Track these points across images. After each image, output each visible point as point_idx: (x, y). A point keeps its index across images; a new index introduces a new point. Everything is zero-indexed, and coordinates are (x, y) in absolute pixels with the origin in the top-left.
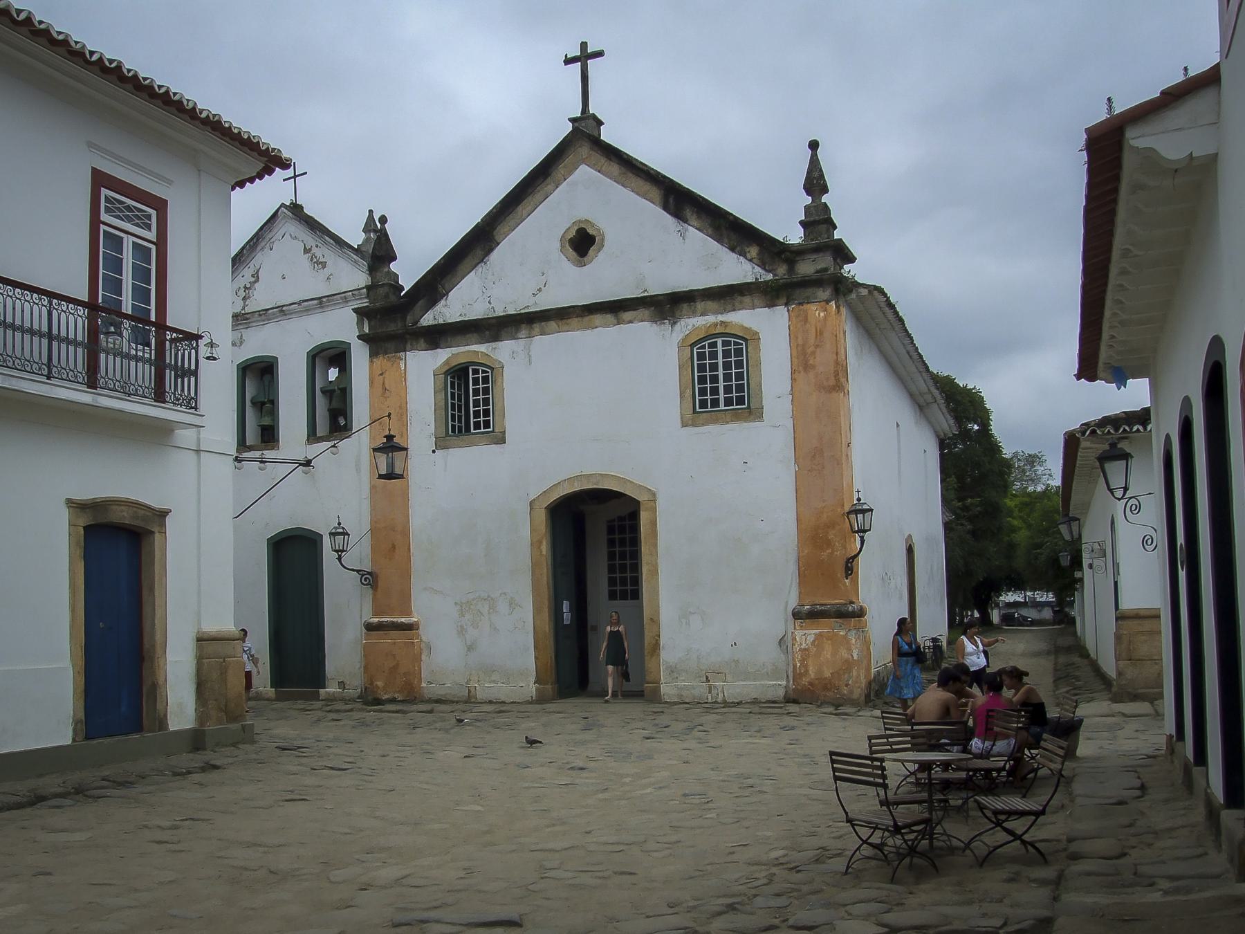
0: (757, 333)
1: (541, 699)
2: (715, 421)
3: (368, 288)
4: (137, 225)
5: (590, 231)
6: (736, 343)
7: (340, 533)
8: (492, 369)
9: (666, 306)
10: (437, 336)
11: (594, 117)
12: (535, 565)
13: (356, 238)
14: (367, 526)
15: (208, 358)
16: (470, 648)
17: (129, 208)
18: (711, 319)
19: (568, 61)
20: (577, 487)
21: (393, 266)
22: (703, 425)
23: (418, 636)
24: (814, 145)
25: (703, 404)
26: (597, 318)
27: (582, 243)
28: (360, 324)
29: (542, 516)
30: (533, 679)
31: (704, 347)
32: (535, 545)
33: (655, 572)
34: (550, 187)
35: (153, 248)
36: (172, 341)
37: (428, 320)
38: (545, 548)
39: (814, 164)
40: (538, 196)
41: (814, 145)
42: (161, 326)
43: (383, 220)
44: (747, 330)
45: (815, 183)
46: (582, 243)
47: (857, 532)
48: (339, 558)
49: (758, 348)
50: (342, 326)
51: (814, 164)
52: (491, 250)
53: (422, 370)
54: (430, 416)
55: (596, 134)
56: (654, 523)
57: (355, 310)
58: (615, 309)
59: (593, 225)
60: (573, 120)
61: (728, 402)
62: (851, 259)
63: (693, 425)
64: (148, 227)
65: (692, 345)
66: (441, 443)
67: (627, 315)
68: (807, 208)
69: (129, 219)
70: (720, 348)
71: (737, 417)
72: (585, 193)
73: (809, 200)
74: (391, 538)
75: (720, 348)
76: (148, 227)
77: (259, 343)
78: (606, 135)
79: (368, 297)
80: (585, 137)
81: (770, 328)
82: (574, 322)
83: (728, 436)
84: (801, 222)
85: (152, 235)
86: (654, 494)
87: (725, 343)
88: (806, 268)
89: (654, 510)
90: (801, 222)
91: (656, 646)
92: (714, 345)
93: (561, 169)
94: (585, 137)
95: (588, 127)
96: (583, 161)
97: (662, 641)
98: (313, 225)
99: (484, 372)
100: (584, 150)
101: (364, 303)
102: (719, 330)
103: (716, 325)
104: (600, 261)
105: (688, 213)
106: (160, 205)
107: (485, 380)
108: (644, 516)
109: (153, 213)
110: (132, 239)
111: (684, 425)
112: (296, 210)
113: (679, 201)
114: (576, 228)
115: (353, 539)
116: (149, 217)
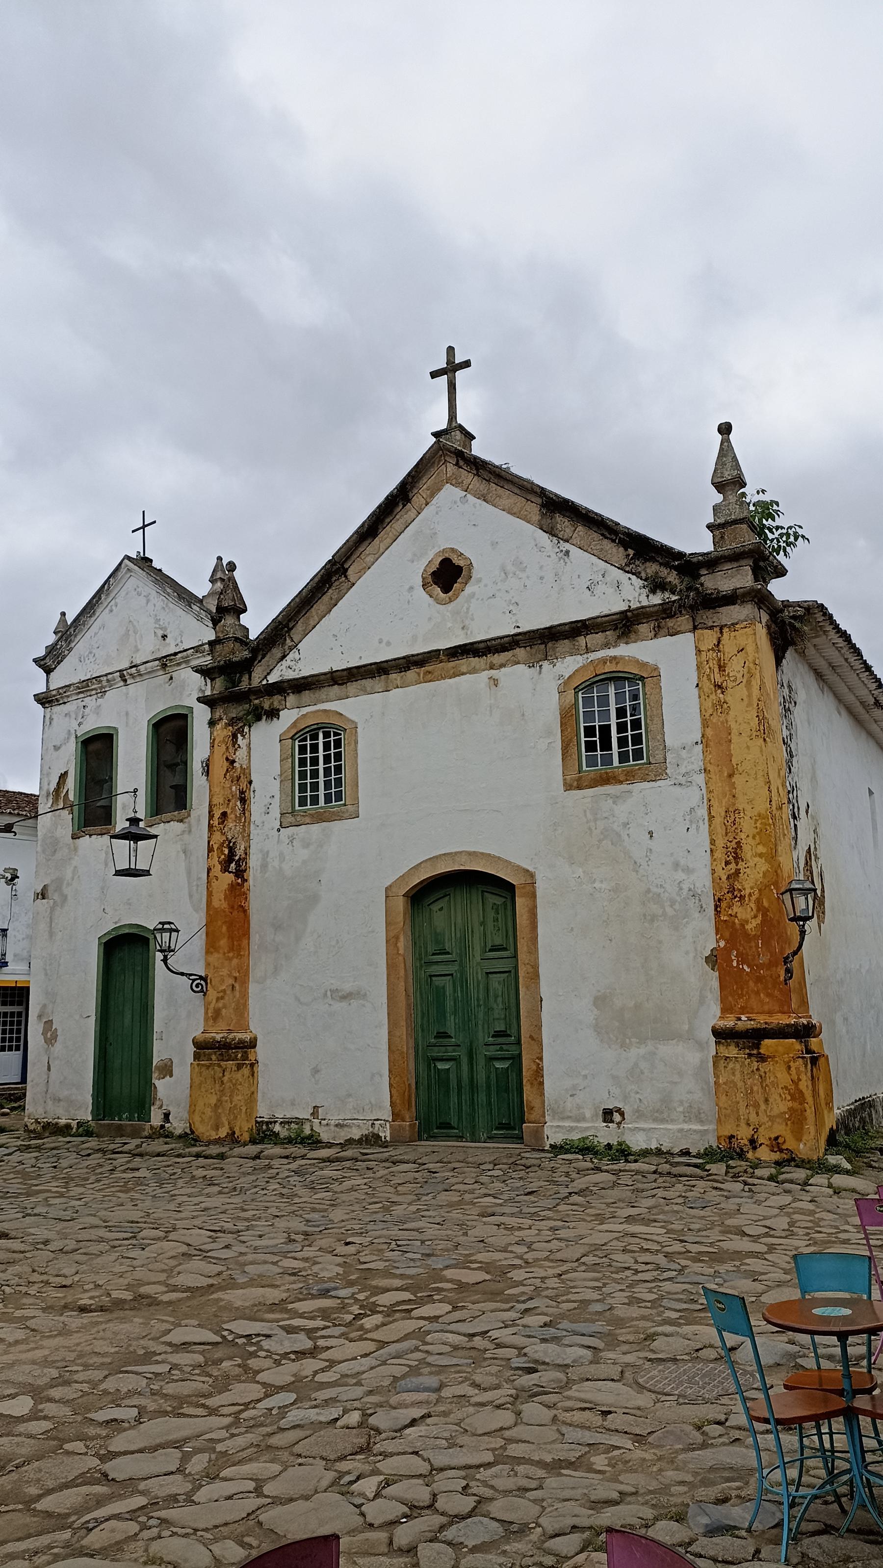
5: (456, 561)
11: (461, 428)
13: (201, 587)
19: (434, 375)
21: (244, 619)
24: (725, 429)
27: (447, 575)
29: (400, 904)
32: (392, 941)
37: (273, 678)
39: (726, 452)
41: (725, 429)
43: (232, 567)
44: (644, 665)
45: (729, 481)
46: (447, 575)
47: (795, 919)
48: (165, 960)
51: (726, 452)
54: (275, 787)
60: (436, 435)
61: (623, 757)
66: (290, 818)
68: (716, 509)
73: (719, 498)
77: (98, 715)
78: (478, 449)
79: (212, 651)
80: (451, 452)
81: (672, 659)
84: (709, 527)
86: (532, 875)
89: (533, 896)
90: (709, 527)
94: (451, 452)
95: (455, 441)
98: (162, 579)
99: (336, 734)
101: (205, 660)
102: (609, 667)
103: (604, 661)
111: (568, 787)
112: (144, 562)
113: (557, 512)
114: (441, 559)
115: (183, 937)
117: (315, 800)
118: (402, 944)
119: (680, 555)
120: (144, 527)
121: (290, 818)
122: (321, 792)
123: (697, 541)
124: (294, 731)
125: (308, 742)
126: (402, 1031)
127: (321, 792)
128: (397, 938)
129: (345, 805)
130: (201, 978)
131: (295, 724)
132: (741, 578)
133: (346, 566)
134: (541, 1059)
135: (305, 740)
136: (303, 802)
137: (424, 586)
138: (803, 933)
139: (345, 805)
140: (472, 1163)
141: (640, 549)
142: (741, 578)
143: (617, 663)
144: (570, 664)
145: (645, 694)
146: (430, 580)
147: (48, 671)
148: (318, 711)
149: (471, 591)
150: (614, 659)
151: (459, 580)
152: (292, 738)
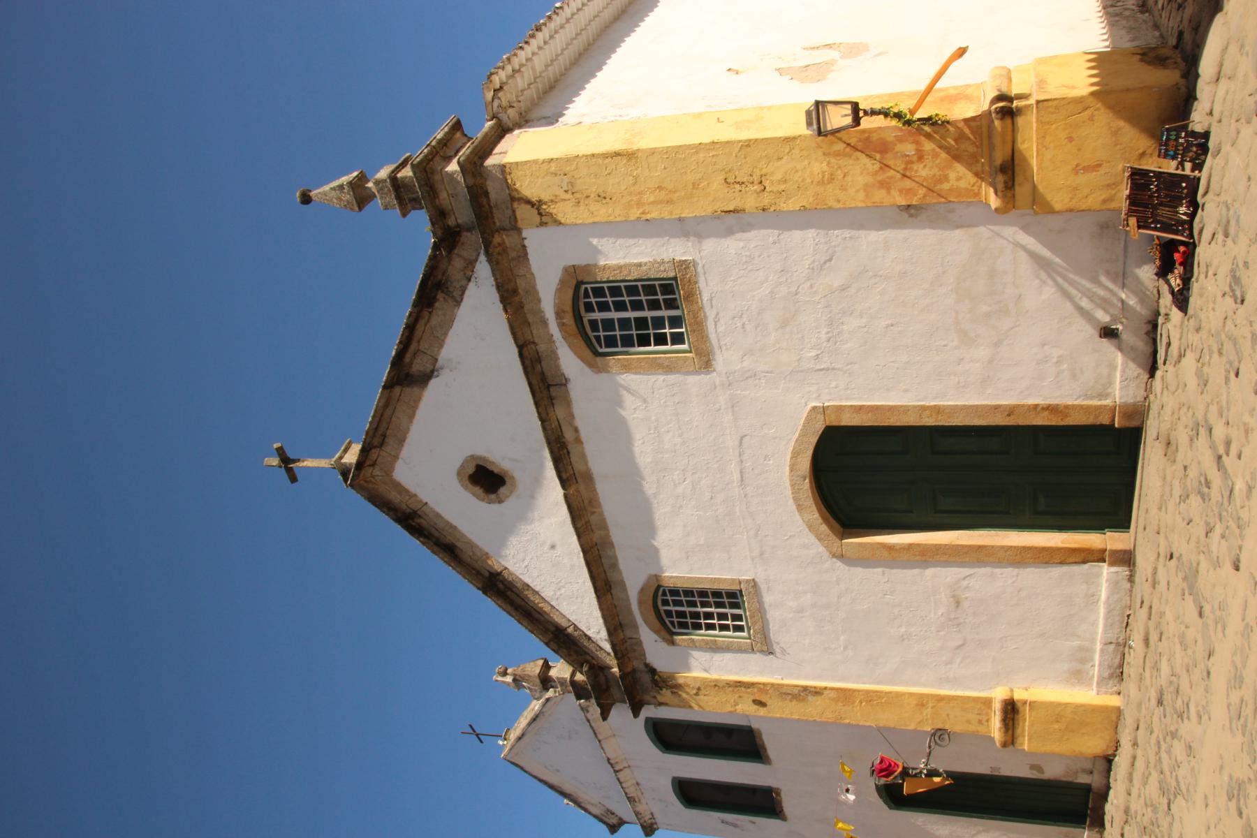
0: (566, 270)
6: (586, 295)
9: (546, 388)
18: (554, 328)
25: (678, 339)
27: (487, 479)
33: (937, 410)
44: (562, 282)
46: (487, 479)
47: (857, 121)
56: (859, 409)
57: (605, 716)
59: (462, 466)
70: (598, 315)
71: (691, 296)
72: (427, 468)
75: (598, 315)
79: (587, 698)
86: (814, 408)
89: (840, 409)
92: (593, 324)
96: (388, 472)
101: (595, 711)
102: (569, 320)
103: (562, 326)
108: (848, 420)
114: (470, 486)
119: (436, 247)
123: (418, 233)
124: (663, 633)
131: (656, 632)
133: (487, 574)
134: (1036, 406)
135: (672, 623)
137: (500, 502)
141: (435, 291)
143: (564, 312)
144: (569, 361)
146: (493, 496)
147: (622, 822)
149: (500, 457)
150: (559, 314)
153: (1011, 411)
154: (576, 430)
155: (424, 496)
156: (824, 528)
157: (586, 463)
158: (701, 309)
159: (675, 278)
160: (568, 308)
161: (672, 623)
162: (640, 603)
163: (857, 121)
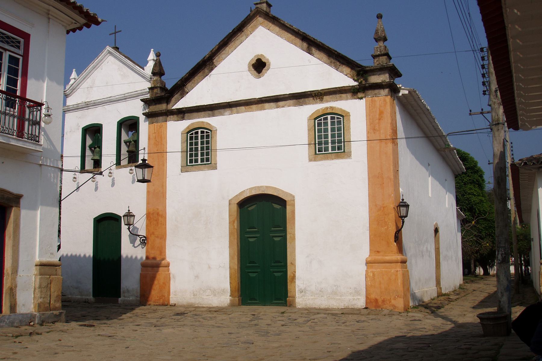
0: (349, 113)
1: (232, 305)
2: (327, 159)
3: (150, 89)
4: (12, 46)
5: (263, 60)
6: (338, 118)
7: (129, 215)
8: (211, 131)
10: (182, 113)
12: (231, 234)
14: (145, 212)
15: (46, 115)
16: (197, 277)
17: (8, 37)
20: (254, 193)
22: (320, 160)
23: (168, 270)
26: (267, 105)
27: (259, 66)
28: (145, 109)
29: (235, 208)
30: (229, 294)
31: (321, 120)
32: (231, 223)
33: (294, 239)
34: (244, 37)
35: (21, 58)
36: (29, 107)
38: (236, 225)
40: (237, 42)
42: (23, 99)
46: (259, 66)
49: (349, 120)
50: (136, 109)
52: (212, 69)
53: (175, 130)
55: (268, 11)
57: (142, 100)
58: (276, 100)
62: (400, 75)
63: (315, 160)
64: (19, 47)
65: (315, 119)
66: (185, 168)
67: (281, 103)
69: (8, 43)
74: (156, 217)
75: (329, 121)
76: (19, 47)
81: (356, 109)
82: (254, 107)
83: (333, 166)
85: (21, 52)
86: (294, 197)
87: (332, 118)
88: (375, 79)
89: (293, 205)
91: (294, 277)
92: (326, 119)
93: (249, 27)
96: (261, 24)
97: (297, 274)
99: (207, 132)
100: (260, 19)
101: (148, 96)
103: (327, 108)
104: (268, 74)
105: (313, 50)
106: (26, 37)
107: (208, 136)
108: (288, 207)
109: (22, 40)
110: (8, 53)
111: (310, 160)
114: (256, 59)
116: (19, 42)
117: (196, 161)
118: (236, 225)
120: (115, 33)
121: (185, 168)
122: (199, 158)
124: (188, 130)
125: (194, 135)
126: (236, 261)
127: (199, 158)
128: (234, 222)
129: (211, 163)
130: (144, 237)
131: (188, 127)
132: (384, 78)
136: (191, 161)
138: (403, 222)
139: (211, 163)
140: (268, 313)
142: (384, 78)
144: (312, 108)
145: (343, 123)
148: (199, 122)
150: (332, 108)
151: (265, 68)
152: (188, 133)
153: (293, 264)
154: (283, 107)
155: (251, 37)
156: (242, 197)
157: (268, 109)
158: (333, 159)
159: (344, 152)
160: (334, 111)
161: (192, 134)
162: (203, 122)
163: (401, 217)
